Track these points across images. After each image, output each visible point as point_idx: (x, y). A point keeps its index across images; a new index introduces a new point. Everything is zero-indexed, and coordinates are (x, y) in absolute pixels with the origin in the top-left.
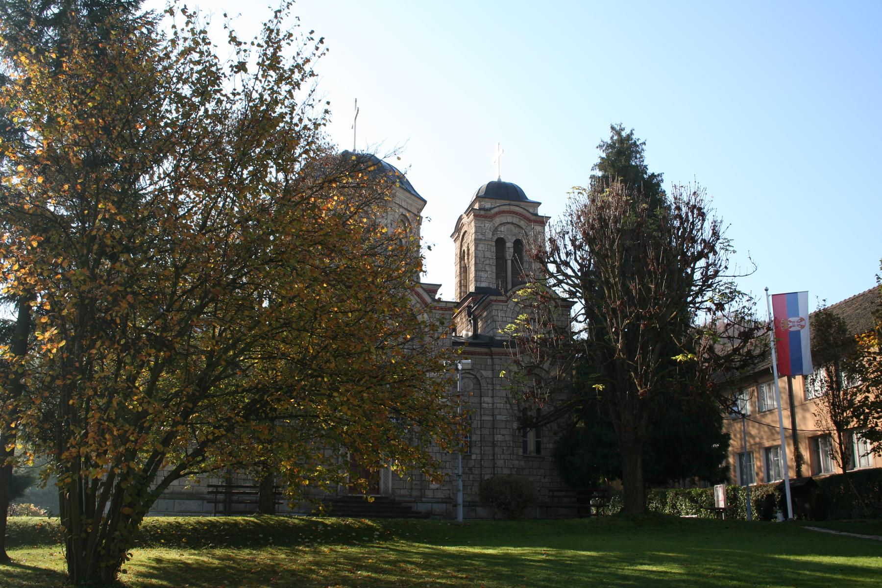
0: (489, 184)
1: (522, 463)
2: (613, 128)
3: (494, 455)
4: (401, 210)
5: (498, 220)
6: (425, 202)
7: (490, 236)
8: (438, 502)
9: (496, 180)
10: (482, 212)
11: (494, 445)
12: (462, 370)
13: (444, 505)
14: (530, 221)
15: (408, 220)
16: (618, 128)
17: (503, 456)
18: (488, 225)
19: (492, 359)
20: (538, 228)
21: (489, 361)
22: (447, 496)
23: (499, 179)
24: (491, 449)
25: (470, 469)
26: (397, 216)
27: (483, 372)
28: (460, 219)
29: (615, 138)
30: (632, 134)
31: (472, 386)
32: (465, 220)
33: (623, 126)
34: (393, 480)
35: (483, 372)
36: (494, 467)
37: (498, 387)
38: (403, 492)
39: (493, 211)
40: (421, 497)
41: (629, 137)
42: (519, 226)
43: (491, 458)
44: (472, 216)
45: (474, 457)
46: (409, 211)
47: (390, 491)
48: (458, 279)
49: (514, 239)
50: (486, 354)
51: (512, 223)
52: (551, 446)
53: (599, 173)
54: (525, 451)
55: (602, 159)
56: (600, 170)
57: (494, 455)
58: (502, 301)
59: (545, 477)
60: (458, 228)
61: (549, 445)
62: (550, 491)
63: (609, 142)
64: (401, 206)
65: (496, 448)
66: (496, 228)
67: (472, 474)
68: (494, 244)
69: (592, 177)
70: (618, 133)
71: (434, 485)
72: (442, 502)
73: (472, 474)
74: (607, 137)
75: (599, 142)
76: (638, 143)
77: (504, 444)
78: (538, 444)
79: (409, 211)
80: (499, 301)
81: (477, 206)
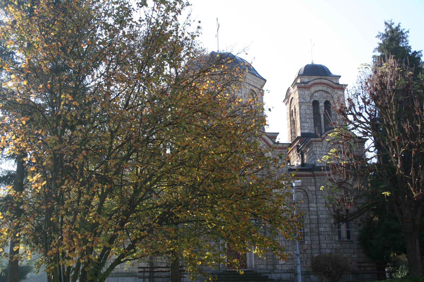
0: (306, 66)
1: (339, 245)
2: (386, 23)
3: (319, 241)
4: (250, 87)
5: (313, 89)
6: (265, 81)
7: (309, 99)
8: (285, 273)
9: (310, 63)
10: (303, 85)
11: (319, 234)
12: (296, 186)
13: (289, 274)
14: (334, 88)
15: (255, 93)
16: (389, 23)
17: (325, 241)
18: (307, 92)
19: (315, 179)
20: (340, 92)
21: (313, 180)
22: (291, 268)
23: (312, 62)
24: (317, 236)
25: (305, 250)
26: (248, 91)
27: (310, 188)
28: (289, 90)
29: (388, 29)
30: (399, 26)
31: (302, 196)
32: (292, 90)
33: (393, 22)
34: (255, 260)
35: (310, 188)
36: (320, 249)
37: (320, 197)
38: (262, 267)
39: (310, 84)
40: (274, 269)
41: (397, 28)
42: (327, 92)
43: (317, 243)
44: (296, 88)
45: (306, 242)
46: (255, 87)
47: (254, 267)
48: (289, 129)
49: (324, 100)
51: (323, 91)
52: (357, 233)
53: (378, 54)
54: (340, 237)
55: (380, 44)
56: (379, 52)
57: (319, 241)
58: (319, 141)
59: (354, 254)
60: (288, 96)
61: (355, 233)
62: (358, 263)
63: (384, 32)
65: (321, 236)
66: (312, 94)
67: (306, 253)
68: (311, 105)
69: (374, 57)
70: (390, 27)
72: (288, 273)
73: (306, 253)
74: (383, 29)
75: (377, 34)
76: (404, 32)
77: (326, 233)
78: (348, 233)
79: (255, 87)
80: (317, 141)
81: (299, 81)
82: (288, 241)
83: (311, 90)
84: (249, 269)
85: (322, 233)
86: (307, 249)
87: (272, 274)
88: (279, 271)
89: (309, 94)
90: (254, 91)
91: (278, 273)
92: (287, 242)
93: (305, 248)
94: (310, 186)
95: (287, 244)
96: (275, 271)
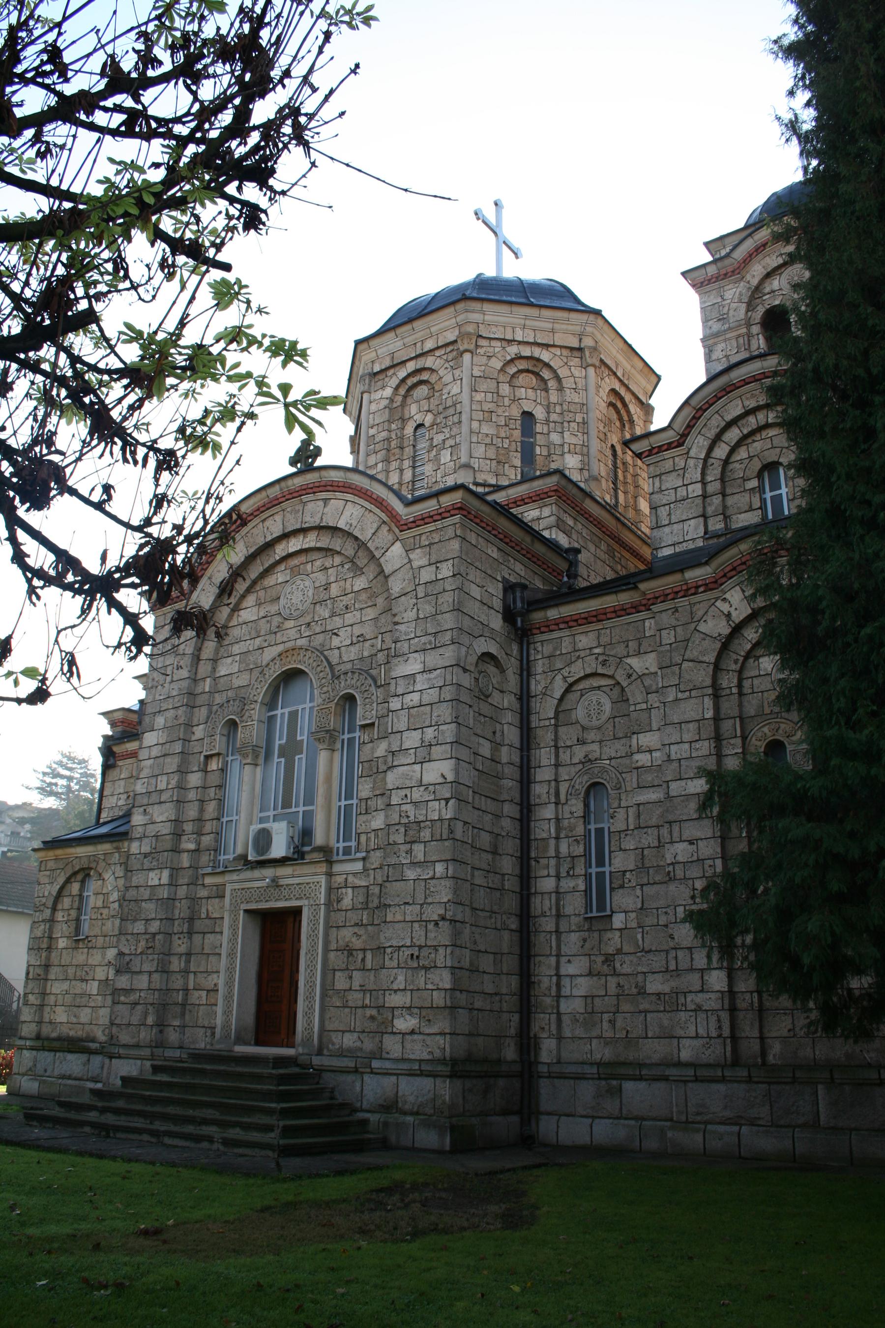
8: (411, 1074)
13: (427, 1083)
15: (547, 365)
22: (438, 1054)
25: (609, 959)
31: (607, 706)
35: (634, 662)
45: (618, 921)
50: (636, 608)
58: (669, 446)
64: (510, 342)
66: (758, 288)
67: (615, 974)
68: (756, 329)
71: (403, 1024)
72: (422, 1074)
73: (615, 974)
82: (436, 924)
83: (748, 277)
84: (300, 1050)
85: (679, 873)
86: (619, 951)
87: (366, 1077)
88: (388, 1065)
89: (741, 294)
90: (538, 360)
91: (387, 1073)
92: (431, 926)
93: (611, 950)
94: (638, 653)
95: (431, 935)
96: (375, 1064)
